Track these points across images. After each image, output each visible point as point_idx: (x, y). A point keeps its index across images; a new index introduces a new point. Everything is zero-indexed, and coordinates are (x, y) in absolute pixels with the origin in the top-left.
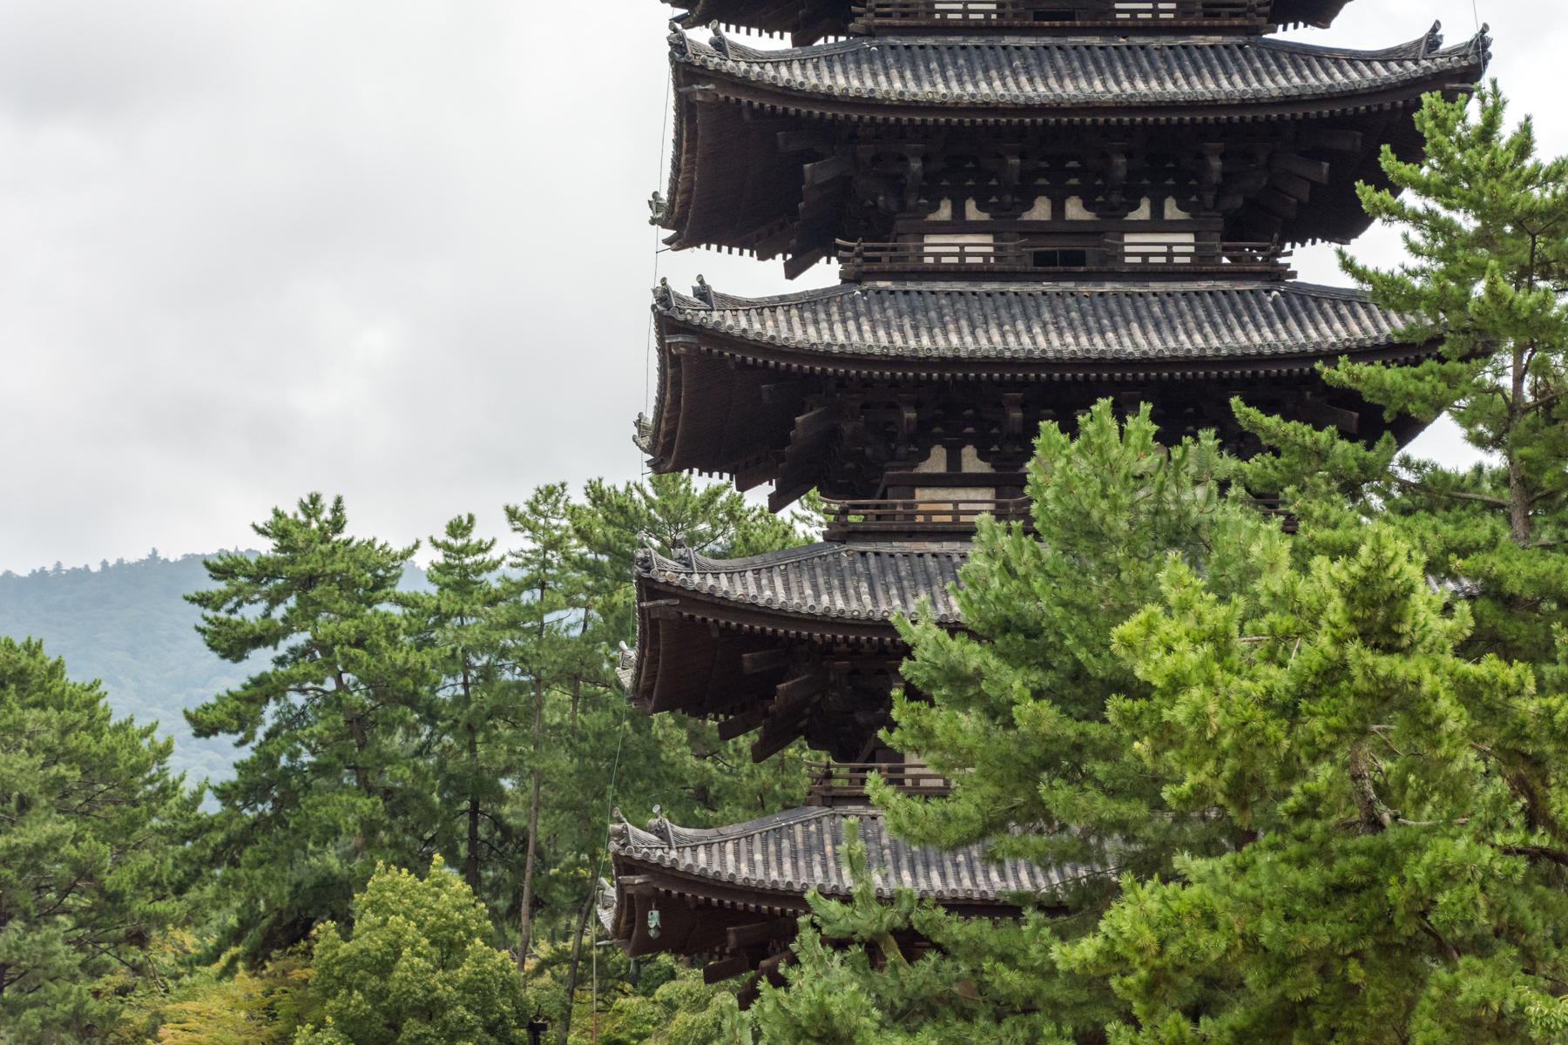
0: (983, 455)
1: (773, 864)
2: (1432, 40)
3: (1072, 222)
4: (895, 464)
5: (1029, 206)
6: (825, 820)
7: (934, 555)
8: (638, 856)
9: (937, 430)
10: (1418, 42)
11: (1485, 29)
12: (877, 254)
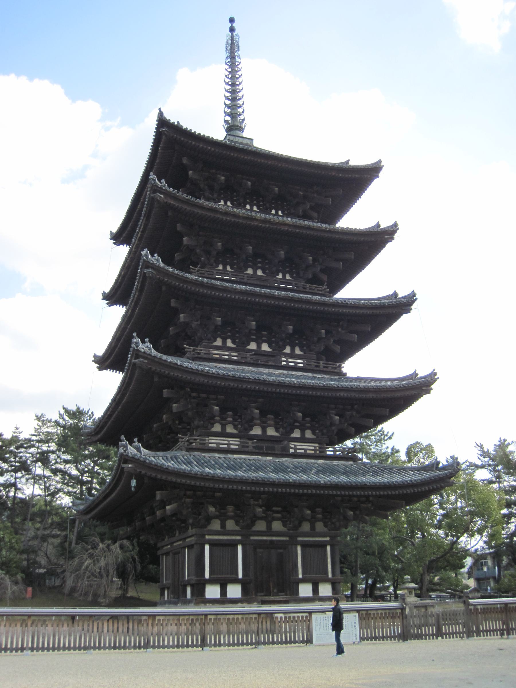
0: (233, 342)
1: (179, 465)
2: (378, 225)
5: (246, 270)
6: (188, 456)
7: (224, 368)
9: (219, 333)
11: (396, 222)
12: (204, 272)
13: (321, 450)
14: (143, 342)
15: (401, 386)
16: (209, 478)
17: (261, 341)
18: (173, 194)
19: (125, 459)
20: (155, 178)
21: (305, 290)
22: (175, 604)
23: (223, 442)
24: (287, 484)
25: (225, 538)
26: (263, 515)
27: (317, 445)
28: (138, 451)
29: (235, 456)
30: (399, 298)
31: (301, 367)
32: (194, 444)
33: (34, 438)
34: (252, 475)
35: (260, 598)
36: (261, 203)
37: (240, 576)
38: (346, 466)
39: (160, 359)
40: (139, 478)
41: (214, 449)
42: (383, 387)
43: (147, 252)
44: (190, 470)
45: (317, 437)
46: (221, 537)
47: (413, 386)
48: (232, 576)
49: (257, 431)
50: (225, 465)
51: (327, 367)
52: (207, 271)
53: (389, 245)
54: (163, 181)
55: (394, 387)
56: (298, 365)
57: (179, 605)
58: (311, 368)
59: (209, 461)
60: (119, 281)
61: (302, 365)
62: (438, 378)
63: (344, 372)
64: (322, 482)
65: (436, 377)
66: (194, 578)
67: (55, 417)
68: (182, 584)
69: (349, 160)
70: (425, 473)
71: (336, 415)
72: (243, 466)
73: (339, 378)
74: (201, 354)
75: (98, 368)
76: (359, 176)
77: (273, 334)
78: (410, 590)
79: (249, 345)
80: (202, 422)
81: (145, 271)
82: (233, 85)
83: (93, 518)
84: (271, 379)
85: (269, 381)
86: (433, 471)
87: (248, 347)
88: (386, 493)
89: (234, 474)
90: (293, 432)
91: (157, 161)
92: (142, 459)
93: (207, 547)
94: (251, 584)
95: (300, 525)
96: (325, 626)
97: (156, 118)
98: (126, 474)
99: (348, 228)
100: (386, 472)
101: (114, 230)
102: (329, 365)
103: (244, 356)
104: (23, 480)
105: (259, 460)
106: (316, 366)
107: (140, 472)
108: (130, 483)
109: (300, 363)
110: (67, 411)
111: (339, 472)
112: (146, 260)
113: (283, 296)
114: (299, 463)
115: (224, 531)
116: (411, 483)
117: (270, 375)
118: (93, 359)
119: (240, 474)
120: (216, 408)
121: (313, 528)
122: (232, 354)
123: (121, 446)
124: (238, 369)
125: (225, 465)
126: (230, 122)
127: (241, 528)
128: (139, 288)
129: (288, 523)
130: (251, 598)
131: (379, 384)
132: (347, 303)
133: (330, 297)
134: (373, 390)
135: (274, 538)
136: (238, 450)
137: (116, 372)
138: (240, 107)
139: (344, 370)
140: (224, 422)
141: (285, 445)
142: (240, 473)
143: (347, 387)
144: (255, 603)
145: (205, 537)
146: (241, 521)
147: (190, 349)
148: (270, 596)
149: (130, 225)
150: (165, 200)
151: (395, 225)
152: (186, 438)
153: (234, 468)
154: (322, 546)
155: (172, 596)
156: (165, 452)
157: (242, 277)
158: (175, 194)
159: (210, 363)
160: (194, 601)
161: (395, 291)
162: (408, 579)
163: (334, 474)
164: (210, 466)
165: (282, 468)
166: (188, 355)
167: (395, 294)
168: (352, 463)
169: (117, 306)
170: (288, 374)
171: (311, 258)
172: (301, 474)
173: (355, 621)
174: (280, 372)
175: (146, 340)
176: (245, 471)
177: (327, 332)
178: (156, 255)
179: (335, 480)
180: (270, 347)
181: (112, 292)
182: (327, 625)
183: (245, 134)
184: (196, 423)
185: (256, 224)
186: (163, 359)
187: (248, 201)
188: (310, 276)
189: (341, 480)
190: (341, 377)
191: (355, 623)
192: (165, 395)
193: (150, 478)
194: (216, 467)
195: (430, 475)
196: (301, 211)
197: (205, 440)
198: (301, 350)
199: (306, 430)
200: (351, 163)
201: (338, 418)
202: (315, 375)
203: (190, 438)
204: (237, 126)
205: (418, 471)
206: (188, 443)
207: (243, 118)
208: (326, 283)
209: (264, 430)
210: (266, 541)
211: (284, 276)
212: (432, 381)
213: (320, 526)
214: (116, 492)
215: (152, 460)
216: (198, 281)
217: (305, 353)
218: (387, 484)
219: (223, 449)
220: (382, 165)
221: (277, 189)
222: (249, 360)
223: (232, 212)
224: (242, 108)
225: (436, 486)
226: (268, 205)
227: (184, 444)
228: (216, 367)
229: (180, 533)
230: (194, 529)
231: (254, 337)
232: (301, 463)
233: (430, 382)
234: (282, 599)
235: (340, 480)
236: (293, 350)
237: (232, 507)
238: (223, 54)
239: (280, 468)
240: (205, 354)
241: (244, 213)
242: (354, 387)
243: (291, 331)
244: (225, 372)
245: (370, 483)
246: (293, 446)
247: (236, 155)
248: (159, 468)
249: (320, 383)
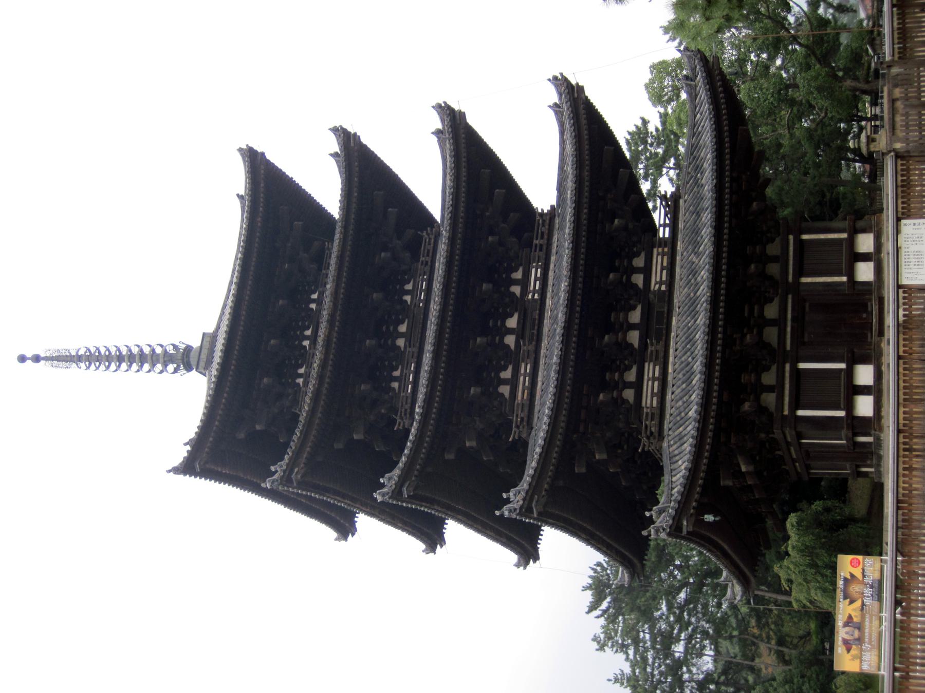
0: (505, 369)
2: (335, 155)
3: (407, 328)
4: (503, 409)
5: (399, 347)
7: (543, 384)
8: (671, 522)
9: (491, 389)
10: (336, 160)
12: (403, 410)
13: (663, 245)
14: (508, 501)
15: (572, 129)
16: (703, 410)
17: (503, 329)
18: (293, 455)
19: (675, 530)
20: (269, 481)
21: (429, 264)
22: (880, 458)
23: (650, 387)
24: (714, 302)
25: (787, 386)
26: (755, 331)
27: (655, 250)
28: (664, 511)
29: (670, 370)
30: (444, 128)
31: (542, 272)
32: (653, 429)
33: (631, 652)
34: (700, 349)
35: (875, 338)
36: (300, 324)
37: (843, 366)
38: (687, 210)
39: (533, 477)
40: (702, 509)
41: (659, 400)
42: (574, 156)
43: (379, 493)
44: (692, 437)
45: (644, 249)
46: (787, 392)
47: (572, 111)
48: (842, 379)
49: (634, 337)
50: (684, 386)
51: (542, 233)
52: (402, 406)
53: (364, 140)
54: (273, 468)
55: (575, 140)
56: (539, 275)
57: (882, 453)
58: (544, 256)
59: (677, 409)
60: (410, 530)
61: (539, 270)
62: (561, 74)
63: (549, 209)
64: (712, 249)
65: (560, 77)
66: (844, 433)
67: (602, 621)
68: (852, 448)
69: (238, 195)
70: (699, 97)
71: (613, 222)
72: (686, 360)
73: (559, 216)
74: (522, 416)
75: (535, 562)
76: (262, 182)
77: (493, 310)
78: (870, 140)
79: (508, 346)
80: (621, 416)
81: (406, 496)
82: (120, 359)
83: (753, 571)
84: (561, 317)
85: (565, 322)
86: (696, 86)
87: (512, 347)
88: (728, 157)
89: (699, 376)
90: (636, 285)
91: (242, 476)
92: (677, 506)
93: (800, 413)
94: (856, 350)
95: (771, 278)
96: (918, 267)
97: (181, 477)
98: (695, 529)
99: (340, 201)
100: (696, 154)
101: (333, 534)
102: (540, 231)
103: (526, 354)
104: (694, 670)
105: (677, 337)
106: (541, 250)
107: (694, 508)
108: (709, 522)
109: (535, 273)
110: (593, 608)
111: (695, 224)
112: (390, 494)
113: (442, 299)
114: (681, 279)
115: (778, 388)
116: (713, 119)
117: (554, 319)
118: (522, 568)
119: (697, 367)
120: (601, 397)
121: (775, 259)
122: (522, 371)
123: (658, 535)
124: (545, 364)
125: (684, 386)
126: (175, 365)
127: (775, 363)
128: (428, 505)
129: (767, 294)
130: (875, 350)
131: (570, 160)
132: (452, 205)
133: (439, 226)
134: (578, 171)
135: (789, 316)
136: (662, 366)
137: (542, 535)
138: (153, 350)
139: (546, 208)
140: (620, 386)
141: (655, 296)
142: (698, 366)
143: (574, 208)
144: (882, 345)
145: (786, 415)
146: (764, 362)
147: (515, 432)
148: (872, 323)
149: (328, 513)
150: (302, 465)
152: (644, 440)
153: (689, 373)
154: (800, 244)
155: (869, 462)
156: (665, 473)
157: (411, 354)
158: (293, 452)
159: (536, 403)
160: (877, 433)
161: (433, 133)
162: (854, 143)
163: (699, 229)
164: (685, 409)
165: (689, 304)
166: (524, 436)
167: (438, 133)
168: (681, 201)
169: (444, 533)
170: (553, 291)
171: (383, 254)
172: (699, 279)
173: (912, 224)
174: (549, 302)
175: (505, 497)
176: (693, 359)
177: (492, 233)
178: (382, 480)
179: (708, 231)
180: (511, 316)
181: (426, 539)
182: (916, 263)
183: (196, 343)
184: (621, 425)
185: (335, 335)
186: (533, 473)
187: (297, 343)
188: (407, 255)
189: (708, 221)
190: (556, 213)
191: (914, 224)
192: (583, 470)
193: (702, 494)
194: (687, 400)
195: (703, 92)
196: (312, 266)
197: (647, 414)
198: (516, 270)
199: (632, 266)
200: (242, 192)
201: (616, 221)
202: (554, 251)
203: (643, 435)
204: (183, 354)
205: (696, 107)
206: (651, 438)
207: (171, 347)
208: (419, 232)
209: (633, 327)
210: (792, 327)
211: (407, 292)
212: (565, 84)
213: (773, 249)
214: (720, 542)
215: (678, 492)
216: (420, 420)
217: (521, 265)
218: (715, 153)
219: (660, 388)
220: (245, 147)
221: (281, 302)
222: (531, 348)
223: (318, 370)
224: (155, 347)
225: (719, 81)
226: (303, 314)
227: (652, 443)
228: (541, 397)
229: (779, 450)
230: (775, 431)
231: (497, 338)
232: (682, 276)
233: (567, 87)
234: (877, 307)
235: (709, 223)
236: (516, 282)
237: (743, 376)
238: (76, 372)
239: (689, 307)
240: (522, 411)
241: (321, 352)
242: (574, 198)
243: (490, 286)
244: (553, 386)
245: (713, 180)
246: (657, 286)
247: (234, 362)
248: (689, 481)
249: (568, 248)
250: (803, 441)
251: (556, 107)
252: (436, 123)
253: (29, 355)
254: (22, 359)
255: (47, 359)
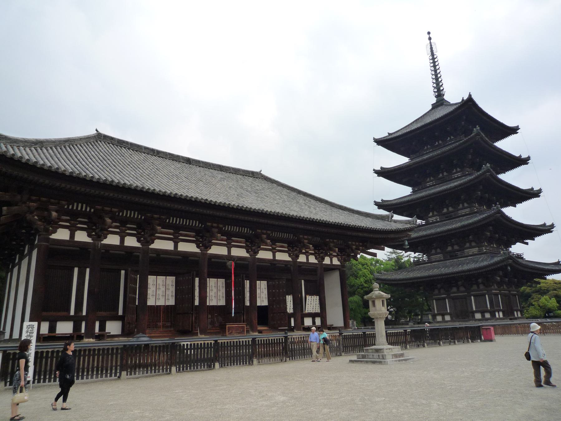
37: (501, 308)
62: (555, 227)
75: (378, 208)
151: (529, 158)
155: (454, 318)
167: (532, 189)
168: (522, 260)
171: (498, 168)
250: (472, 297)
251: (544, 225)
252: (536, 189)
253: (430, 35)
254: (429, 33)
255: (430, 43)
